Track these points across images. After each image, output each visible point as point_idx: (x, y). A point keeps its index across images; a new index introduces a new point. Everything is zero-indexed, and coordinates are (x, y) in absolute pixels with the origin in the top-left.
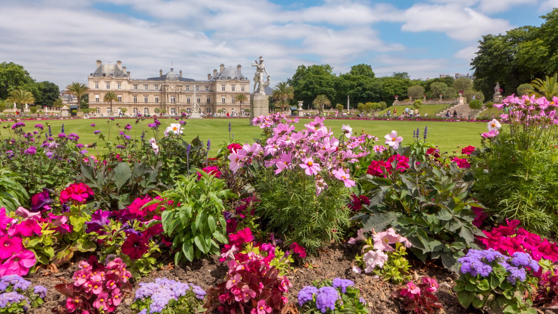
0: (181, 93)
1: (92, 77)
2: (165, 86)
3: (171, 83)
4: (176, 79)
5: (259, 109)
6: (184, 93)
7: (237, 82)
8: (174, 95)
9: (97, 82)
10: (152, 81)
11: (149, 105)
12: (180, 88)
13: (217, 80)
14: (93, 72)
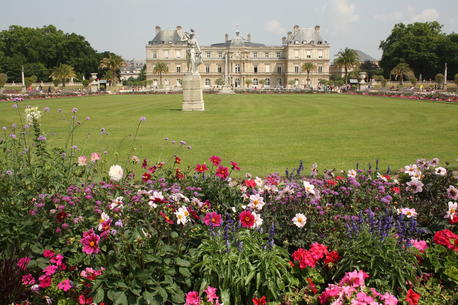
0: (247, 61)
1: (150, 46)
2: (229, 53)
3: (235, 49)
4: (242, 45)
5: (189, 91)
6: (250, 61)
7: (314, 46)
8: (239, 63)
9: (155, 51)
10: (215, 48)
11: (211, 76)
12: (246, 55)
13: (290, 45)
14: (151, 40)
